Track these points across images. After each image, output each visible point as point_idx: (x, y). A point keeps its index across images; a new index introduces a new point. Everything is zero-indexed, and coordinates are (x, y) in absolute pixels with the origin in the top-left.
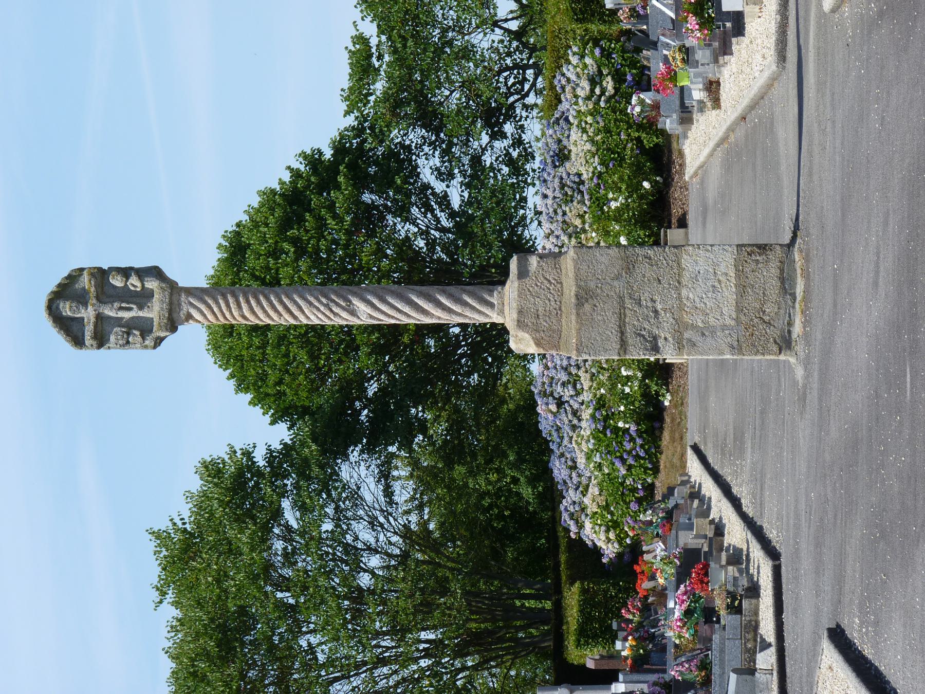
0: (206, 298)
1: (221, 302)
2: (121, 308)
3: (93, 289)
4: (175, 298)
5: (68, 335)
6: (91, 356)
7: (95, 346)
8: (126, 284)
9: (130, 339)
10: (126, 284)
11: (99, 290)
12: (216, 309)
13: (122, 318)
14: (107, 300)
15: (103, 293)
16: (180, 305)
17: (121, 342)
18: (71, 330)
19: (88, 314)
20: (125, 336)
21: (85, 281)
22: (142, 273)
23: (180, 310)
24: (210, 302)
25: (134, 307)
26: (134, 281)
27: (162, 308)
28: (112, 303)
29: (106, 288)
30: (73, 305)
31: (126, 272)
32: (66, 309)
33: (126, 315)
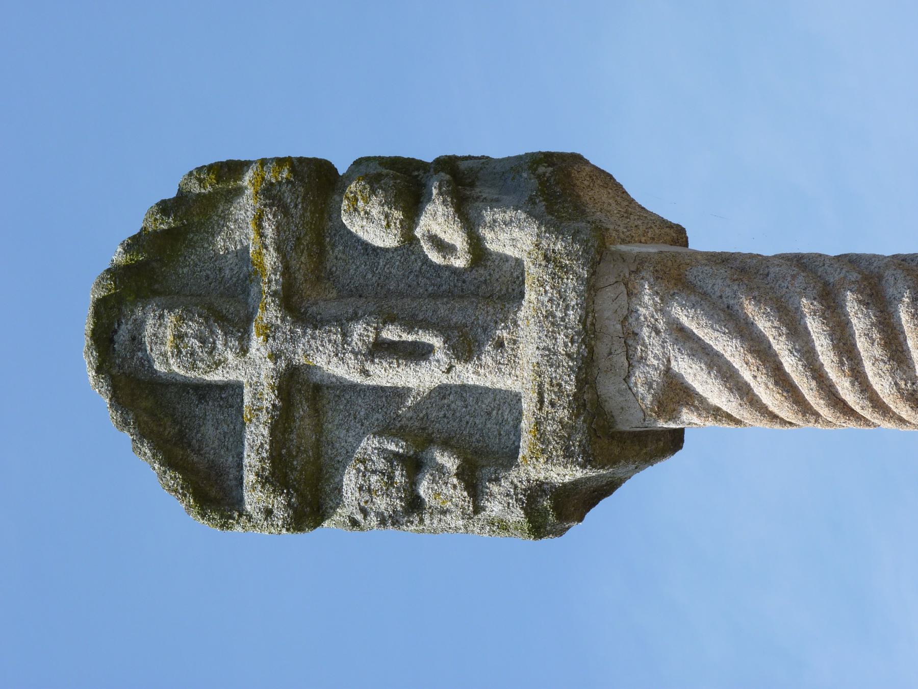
0: (750, 309)
1: (814, 326)
2: (381, 349)
3: (270, 259)
4: (609, 303)
5: (170, 462)
6: (260, 544)
7: (280, 514)
8: (409, 239)
9: (424, 489)
10: (409, 239)
11: (302, 263)
12: (790, 363)
13: (398, 394)
14: (333, 309)
15: (321, 274)
16: (630, 337)
17: (381, 503)
18: (177, 429)
19: (250, 369)
20: (399, 477)
21: (247, 231)
22: (467, 182)
23: (632, 361)
24: (765, 325)
25: (436, 342)
26: (438, 221)
27: (549, 353)
28: (343, 322)
29: (335, 255)
30: (191, 328)
31: (405, 182)
32: (167, 343)
33: (419, 378)
